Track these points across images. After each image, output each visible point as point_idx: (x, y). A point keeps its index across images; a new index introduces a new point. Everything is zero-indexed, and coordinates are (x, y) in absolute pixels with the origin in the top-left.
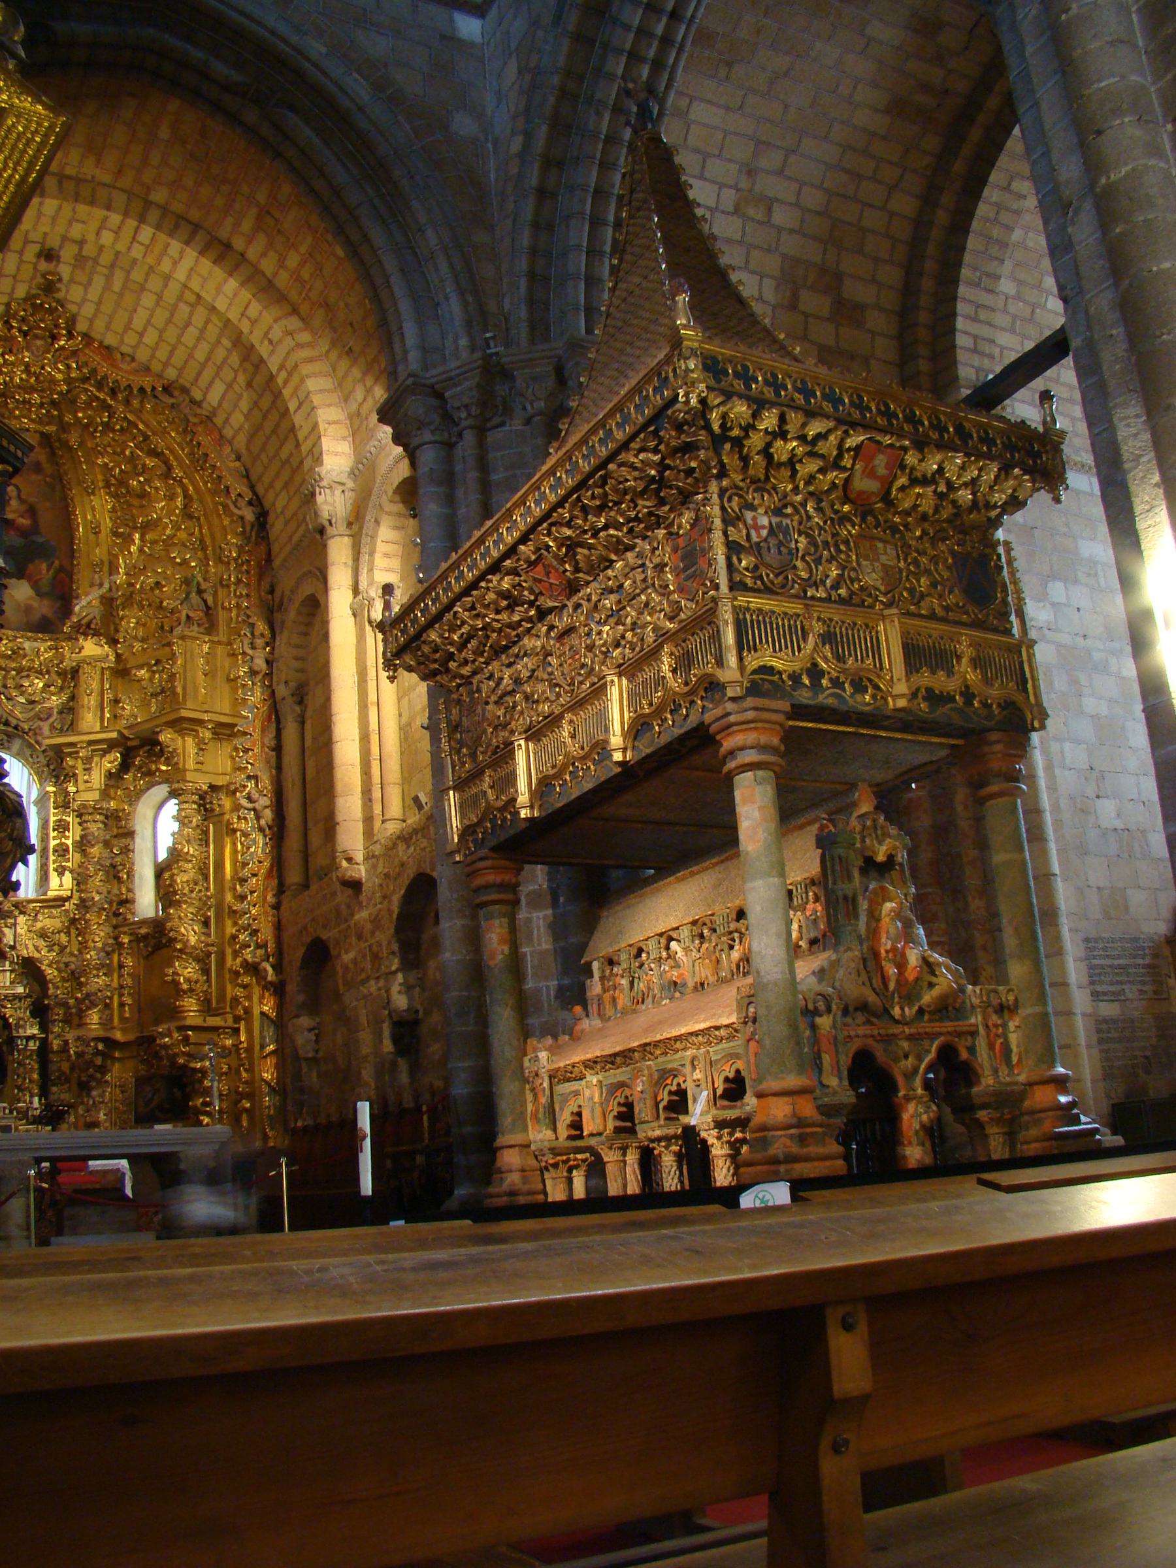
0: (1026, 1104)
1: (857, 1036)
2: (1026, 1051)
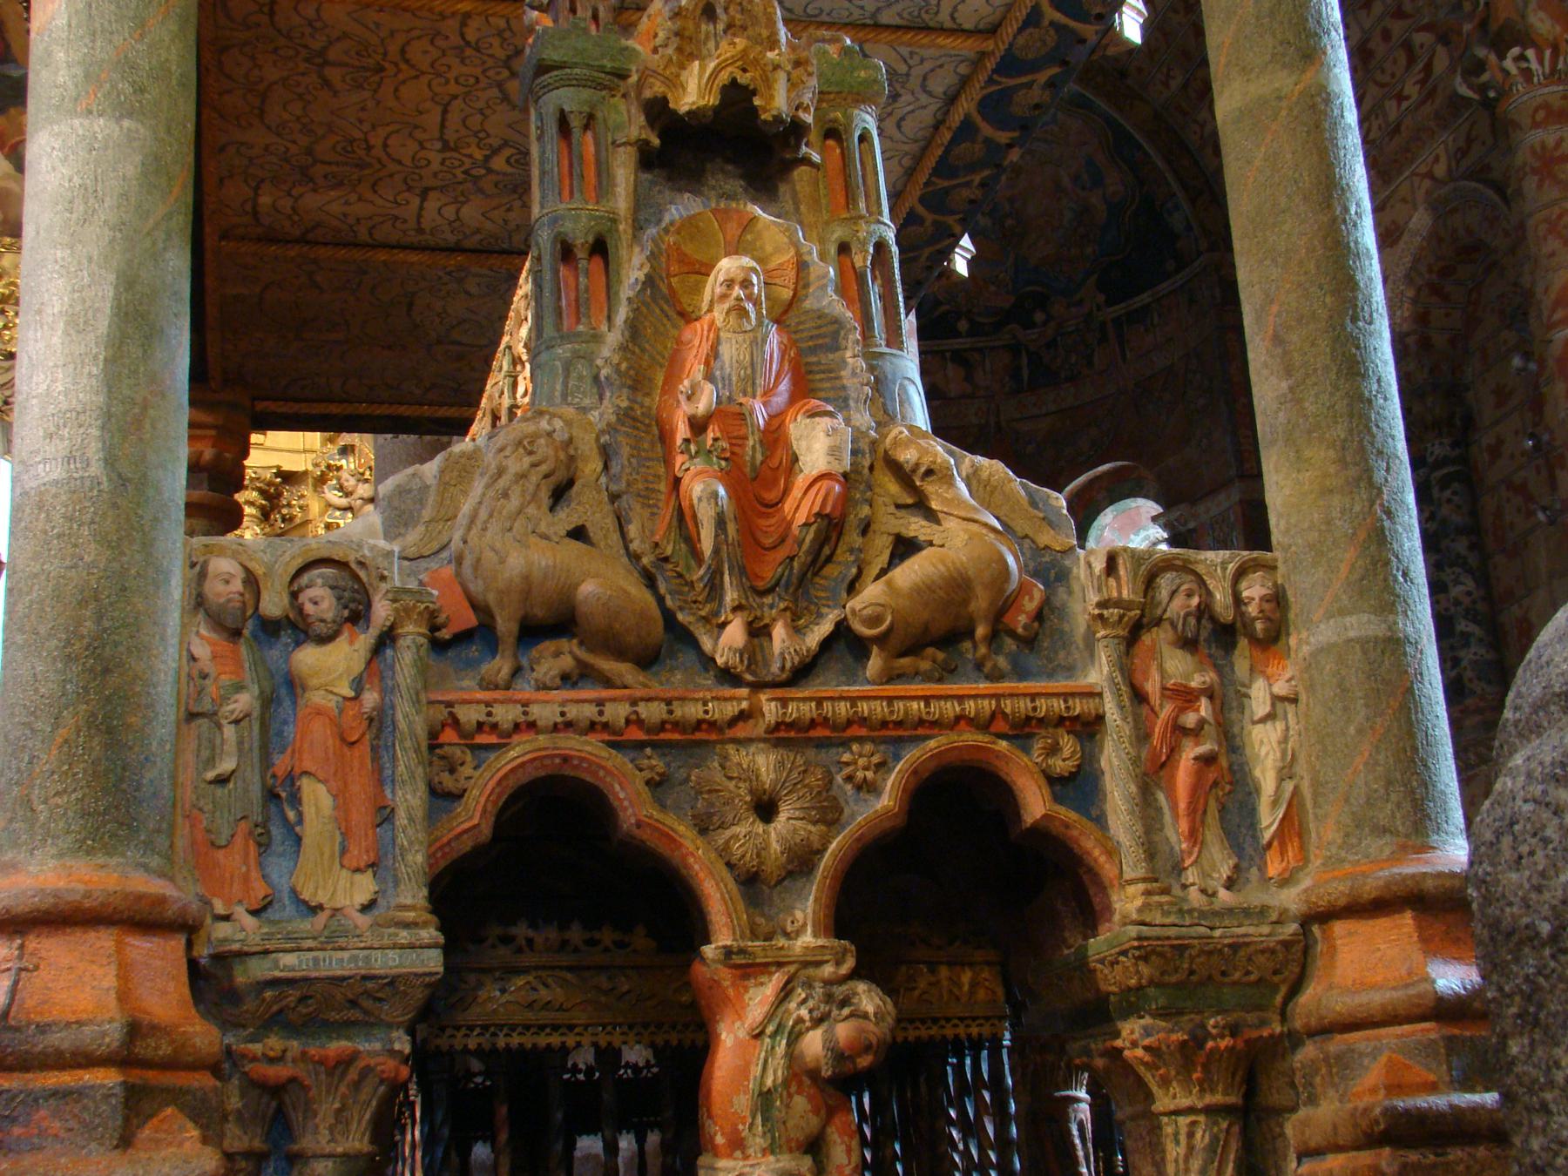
0: (1317, 999)
1: (532, 726)
2: (1316, 784)
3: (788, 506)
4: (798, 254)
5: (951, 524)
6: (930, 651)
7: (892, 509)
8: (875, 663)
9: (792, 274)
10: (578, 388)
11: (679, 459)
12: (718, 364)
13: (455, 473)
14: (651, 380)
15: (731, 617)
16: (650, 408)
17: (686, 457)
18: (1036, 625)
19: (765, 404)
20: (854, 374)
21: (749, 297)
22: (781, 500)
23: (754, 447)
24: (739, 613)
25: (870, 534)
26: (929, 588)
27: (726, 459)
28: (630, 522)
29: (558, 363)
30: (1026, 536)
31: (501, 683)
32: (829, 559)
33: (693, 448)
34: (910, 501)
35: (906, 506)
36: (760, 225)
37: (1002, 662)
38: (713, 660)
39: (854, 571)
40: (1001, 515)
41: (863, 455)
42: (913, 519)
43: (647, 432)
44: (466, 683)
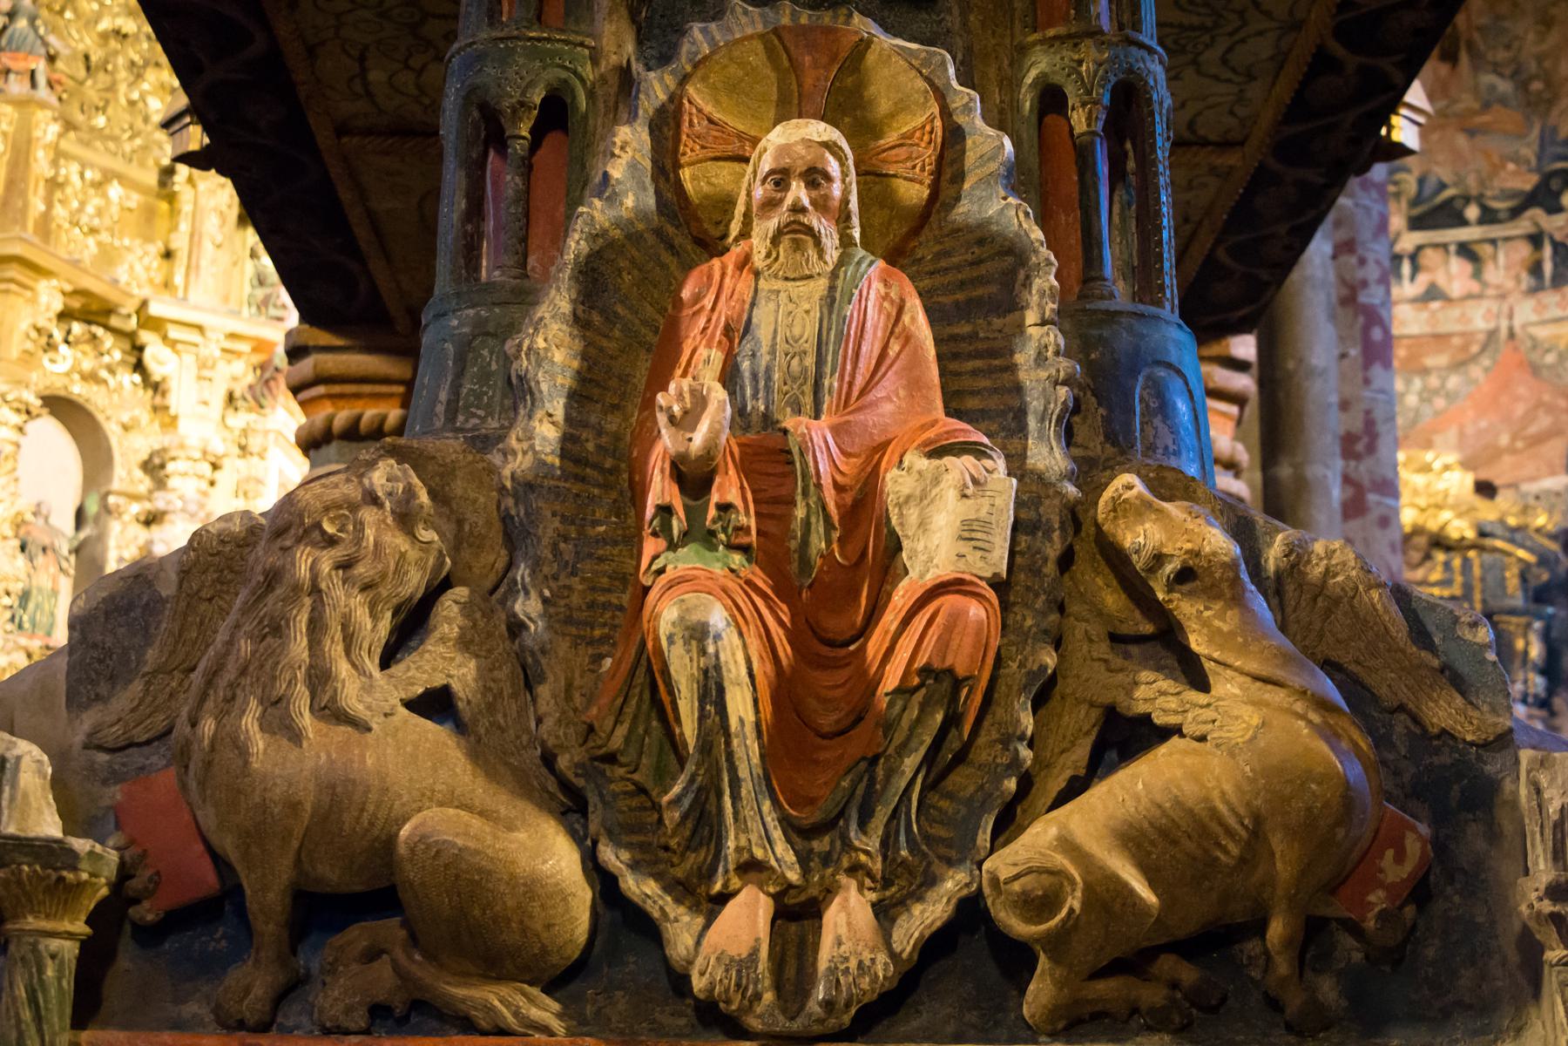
3: (875, 645)
4: (946, 113)
5: (1226, 687)
6: (1167, 964)
7: (1103, 649)
8: (1040, 993)
9: (928, 155)
10: (479, 396)
11: (650, 546)
12: (747, 347)
13: (211, 576)
14: (624, 379)
15: (735, 882)
16: (617, 437)
17: (662, 543)
18: (1410, 911)
19: (837, 430)
20: (1040, 359)
21: (821, 205)
22: (864, 631)
23: (807, 524)
24: (753, 875)
25: (1054, 702)
26: (1163, 833)
27: (745, 549)
28: (542, 679)
29: (449, 346)
30: (1402, 708)
31: (251, 1019)
32: (961, 757)
33: (677, 526)
34: (1148, 628)
35: (1140, 639)
36: (871, 57)
37: (1328, 990)
38: (686, 978)
39: (1011, 784)
40: (1345, 659)
41: (1048, 534)
42: (1145, 675)
43: (606, 487)
44: (192, 1008)
